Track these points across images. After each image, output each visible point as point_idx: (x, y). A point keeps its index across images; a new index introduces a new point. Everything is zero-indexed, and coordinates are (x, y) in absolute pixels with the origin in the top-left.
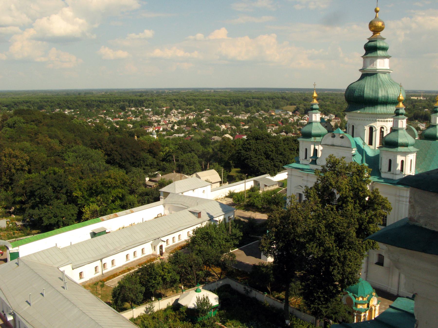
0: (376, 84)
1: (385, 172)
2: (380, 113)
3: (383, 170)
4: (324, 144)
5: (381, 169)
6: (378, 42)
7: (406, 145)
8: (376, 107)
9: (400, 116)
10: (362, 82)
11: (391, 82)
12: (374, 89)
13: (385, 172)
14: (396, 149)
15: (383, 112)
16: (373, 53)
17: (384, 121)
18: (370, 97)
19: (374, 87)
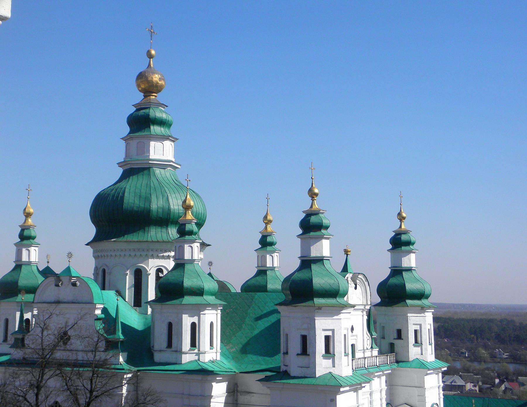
0: (148, 186)
1: (160, 351)
2: (154, 239)
3: (157, 347)
4: (39, 301)
5: (153, 347)
6: (151, 110)
7: (199, 292)
8: (147, 229)
9: (187, 237)
10: (123, 184)
11: (177, 185)
12: (143, 194)
13: (160, 351)
14: (180, 300)
15: (160, 239)
16: (143, 130)
17: (163, 257)
18: (135, 209)
19: (143, 191)
